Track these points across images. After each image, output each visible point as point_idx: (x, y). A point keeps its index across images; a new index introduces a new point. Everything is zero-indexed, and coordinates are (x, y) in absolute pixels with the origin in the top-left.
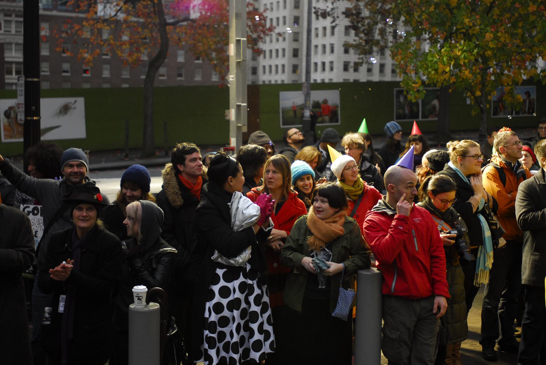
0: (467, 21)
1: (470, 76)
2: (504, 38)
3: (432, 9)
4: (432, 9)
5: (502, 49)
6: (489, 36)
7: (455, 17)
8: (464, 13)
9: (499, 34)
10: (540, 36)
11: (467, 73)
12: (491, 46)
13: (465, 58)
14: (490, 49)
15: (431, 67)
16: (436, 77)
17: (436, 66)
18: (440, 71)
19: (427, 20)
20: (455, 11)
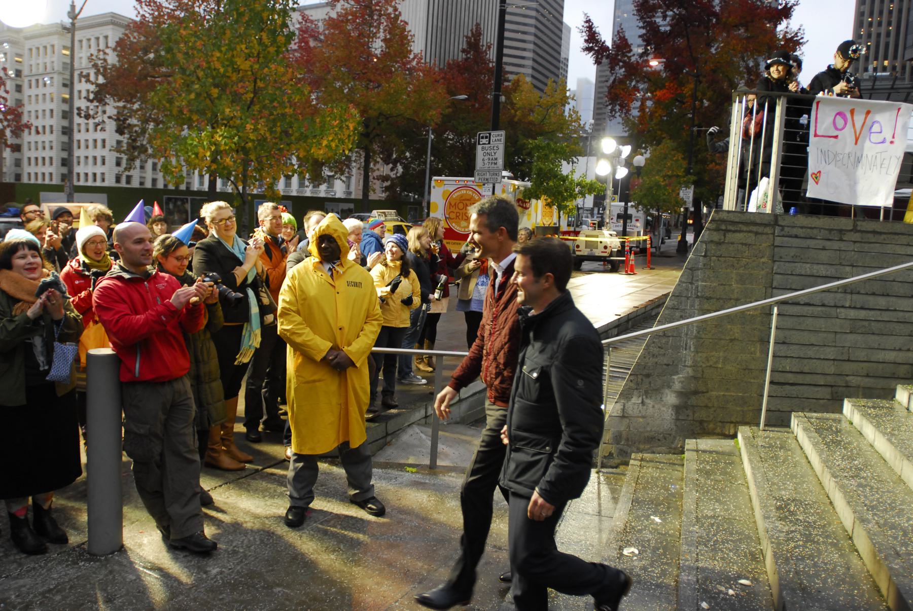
0: (227, 110)
1: (232, 163)
2: (263, 130)
3: (193, 96)
4: (193, 96)
5: (262, 141)
6: (249, 127)
7: (216, 107)
8: (224, 102)
9: (259, 126)
10: (297, 134)
11: (228, 161)
12: (252, 138)
13: (226, 144)
14: (253, 141)
15: (191, 151)
16: (197, 161)
17: (196, 150)
18: (200, 155)
19: (187, 106)
20: (216, 101)
